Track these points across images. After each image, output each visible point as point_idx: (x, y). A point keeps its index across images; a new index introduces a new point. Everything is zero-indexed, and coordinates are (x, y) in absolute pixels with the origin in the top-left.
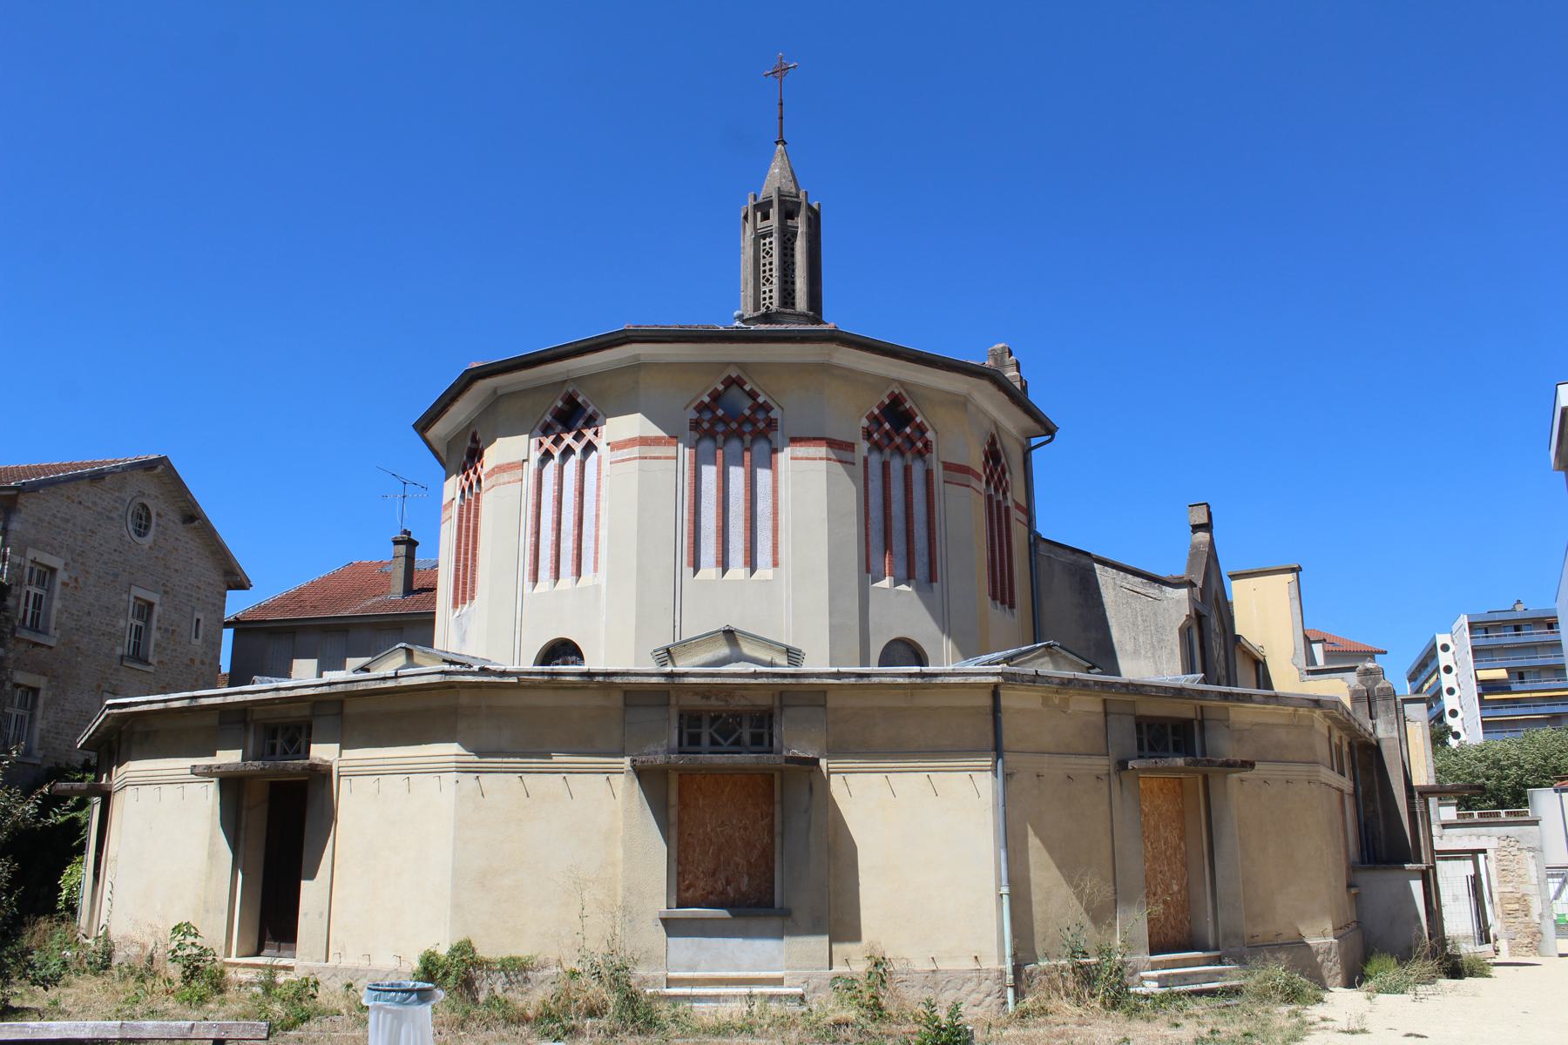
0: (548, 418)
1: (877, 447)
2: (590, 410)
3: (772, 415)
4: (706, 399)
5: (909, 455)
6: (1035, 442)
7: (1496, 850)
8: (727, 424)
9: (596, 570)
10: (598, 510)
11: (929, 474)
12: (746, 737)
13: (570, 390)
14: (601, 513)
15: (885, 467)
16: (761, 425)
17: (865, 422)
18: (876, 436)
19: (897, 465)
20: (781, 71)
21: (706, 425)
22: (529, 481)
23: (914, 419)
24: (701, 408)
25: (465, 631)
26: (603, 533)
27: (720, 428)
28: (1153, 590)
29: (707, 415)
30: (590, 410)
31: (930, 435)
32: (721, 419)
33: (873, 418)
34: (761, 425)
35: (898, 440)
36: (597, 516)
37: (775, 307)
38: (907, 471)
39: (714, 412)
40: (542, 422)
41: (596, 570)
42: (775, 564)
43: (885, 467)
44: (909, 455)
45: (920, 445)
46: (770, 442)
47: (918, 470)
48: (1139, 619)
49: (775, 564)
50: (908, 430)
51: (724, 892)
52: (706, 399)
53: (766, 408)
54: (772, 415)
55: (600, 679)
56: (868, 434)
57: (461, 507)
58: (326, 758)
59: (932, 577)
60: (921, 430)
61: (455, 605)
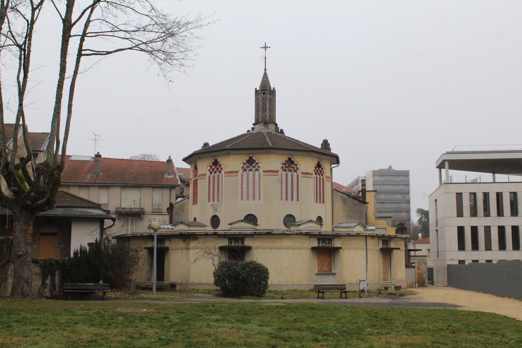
0: (245, 162)
1: (316, 174)
2: (257, 161)
3: (298, 166)
4: (284, 162)
5: (321, 175)
6: (333, 166)
7: (418, 263)
8: (288, 168)
9: (260, 199)
10: (260, 185)
11: (323, 179)
12: (327, 243)
13: (251, 156)
14: (261, 186)
15: (317, 178)
16: (295, 169)
17: (314, 168)
18: (316, 171)
19: (318, 177)
20: (265, 48)
21: (284, 168)
22: (240, 176)
23: (321, 166)
24: (283, 164)
25: (217, 209)
26: (262, 191)
27: (287, 169)
28: (360, 204)
29: (284, 166)
30: (257, 161)
31: (324, 170)
32: (287, 167)
33: (316, 168)
34: (295, 169)
35: (319, 172)
36: (260, 187)
37: (268, 120)
38: (320, 178)
39: (286, 165)
40: (243, 162)
41: (260, 199)
42: (298, 200)
43: (317, 178)
44: (321, 175)
45: (322, 172)
46: (297, 172)
47: (322, 177)
48: (357, 210)
49: (298, 200)
50: (321, 169)
51: (323, 270)
52: (284, 162)
53: (296, 165)
54: (298, 166)
55: (308, 233)
56: (315, 171)
57: (209, 177)
58: (250, 245)
59: (323, 203)
60: (322, 169)
61: (209, 201)
